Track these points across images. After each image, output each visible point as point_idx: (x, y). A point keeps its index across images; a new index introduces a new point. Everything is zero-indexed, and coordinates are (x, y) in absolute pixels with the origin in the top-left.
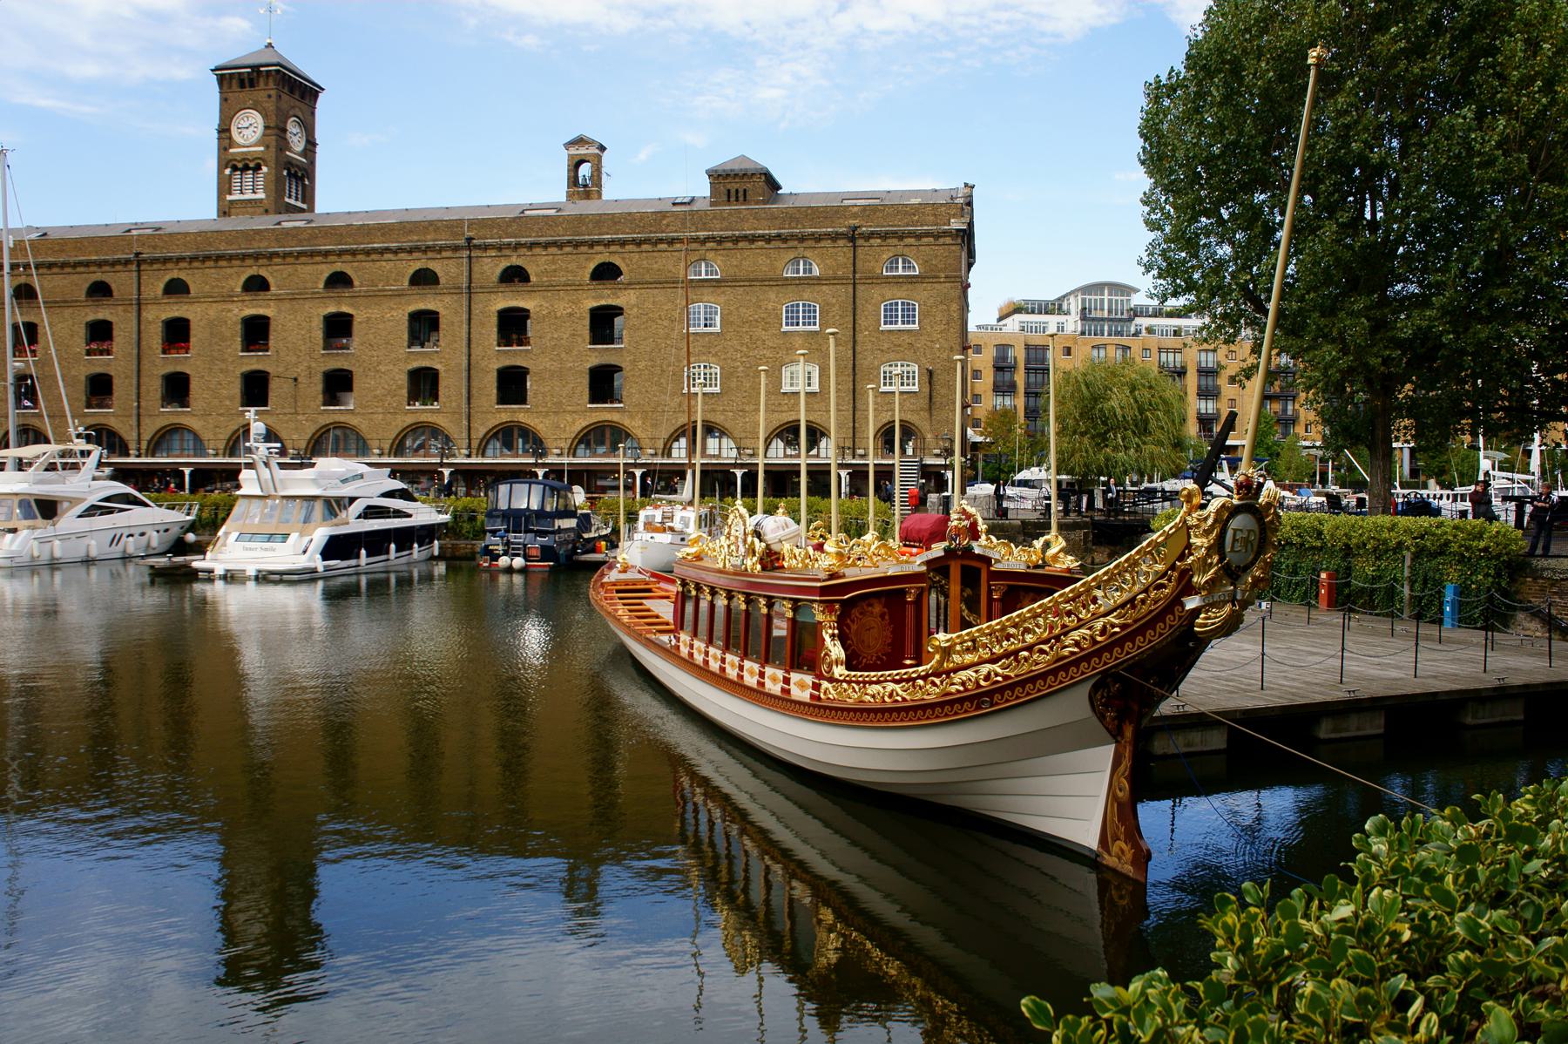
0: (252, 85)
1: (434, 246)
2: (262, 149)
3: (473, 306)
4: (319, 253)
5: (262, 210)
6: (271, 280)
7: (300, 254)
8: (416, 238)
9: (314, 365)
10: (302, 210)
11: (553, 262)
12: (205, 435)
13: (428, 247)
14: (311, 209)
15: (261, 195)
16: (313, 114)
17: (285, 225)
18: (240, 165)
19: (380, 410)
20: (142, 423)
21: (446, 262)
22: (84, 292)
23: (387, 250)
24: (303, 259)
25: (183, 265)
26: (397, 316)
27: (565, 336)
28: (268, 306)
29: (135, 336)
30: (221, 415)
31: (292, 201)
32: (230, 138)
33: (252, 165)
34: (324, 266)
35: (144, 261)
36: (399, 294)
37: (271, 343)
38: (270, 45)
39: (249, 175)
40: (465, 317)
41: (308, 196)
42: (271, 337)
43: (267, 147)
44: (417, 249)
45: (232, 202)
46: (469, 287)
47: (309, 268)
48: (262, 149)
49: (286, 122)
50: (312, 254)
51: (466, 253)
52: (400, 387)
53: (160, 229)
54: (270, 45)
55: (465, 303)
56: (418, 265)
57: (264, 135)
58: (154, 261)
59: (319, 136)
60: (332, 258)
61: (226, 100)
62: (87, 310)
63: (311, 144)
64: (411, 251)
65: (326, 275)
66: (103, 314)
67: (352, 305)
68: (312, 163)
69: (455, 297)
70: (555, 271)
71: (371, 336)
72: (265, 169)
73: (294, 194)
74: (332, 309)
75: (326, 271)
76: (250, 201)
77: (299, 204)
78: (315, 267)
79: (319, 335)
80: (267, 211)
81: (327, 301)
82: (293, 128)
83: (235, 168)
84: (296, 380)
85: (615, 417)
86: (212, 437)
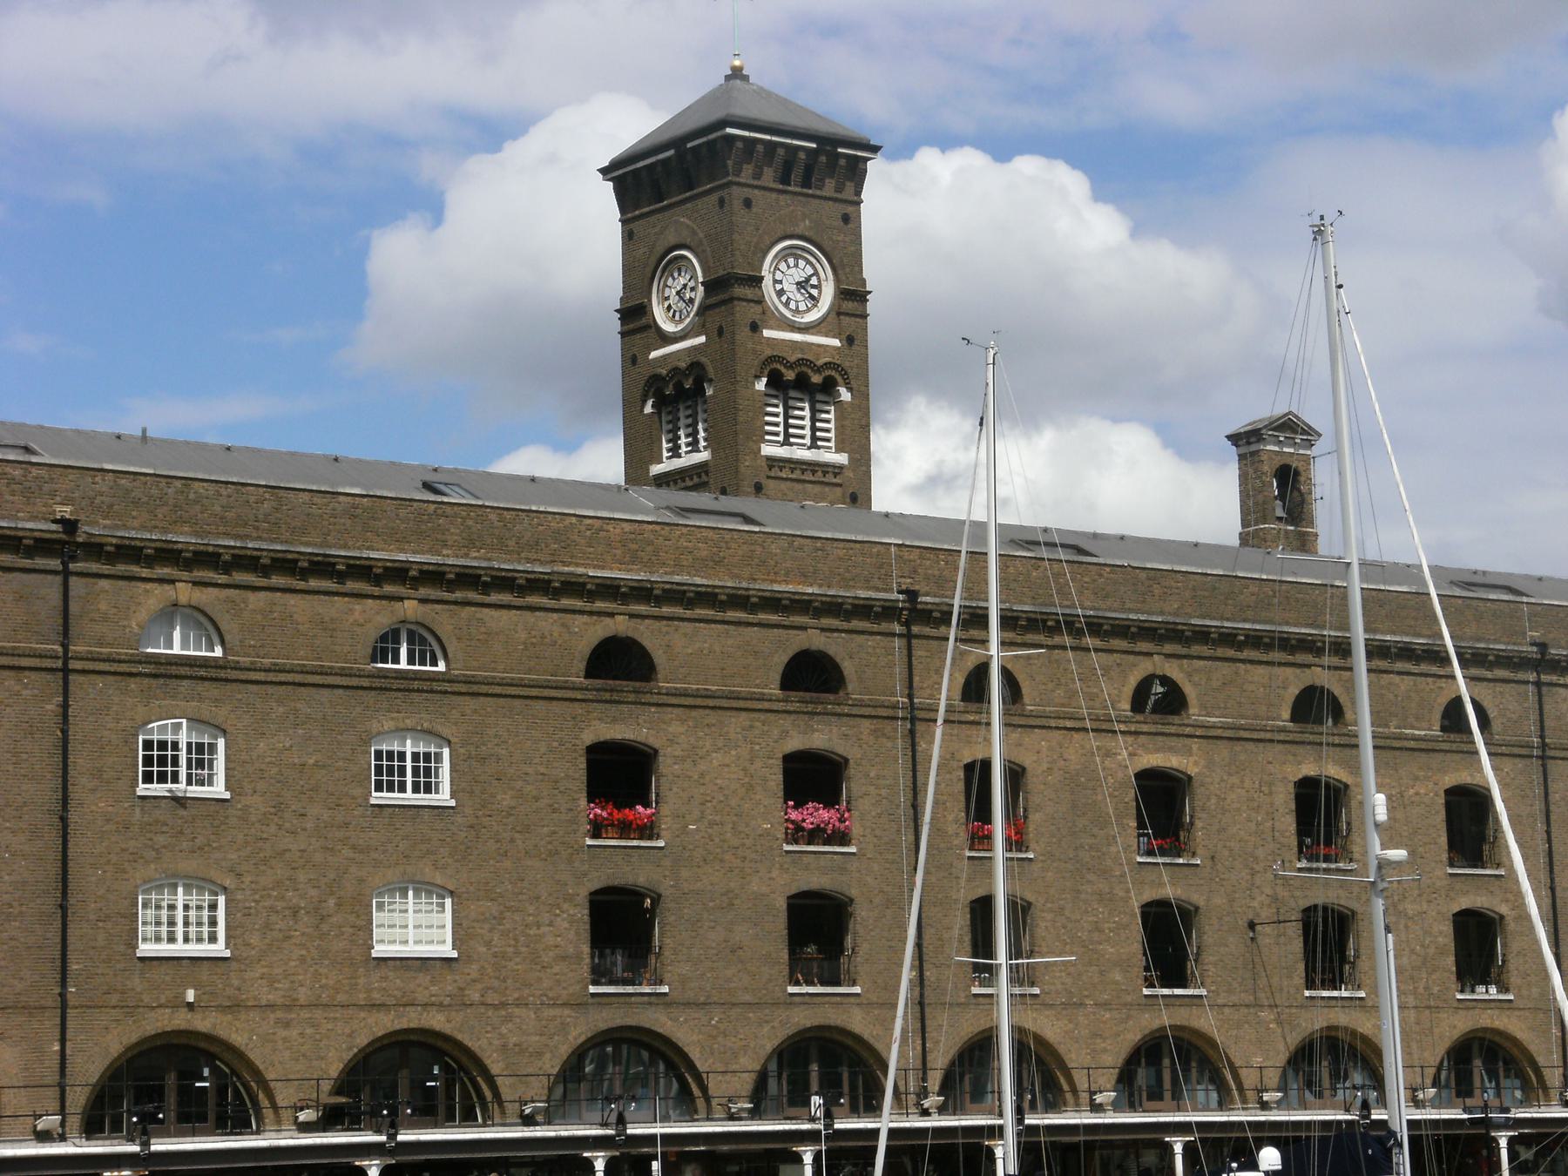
0: (806, 183)
2: (836, 342)
3: (1552, 787)
6: (1189, 690)
18: (790, 375)
21: (1499, 687)
22: (776, 677)
29: (903, 799)
30: (1105, 1005)
32: (760, 301)
33: (816, 379)
38: (737, 74)
45: (772, 461)
46: (1544, 746)
48: (836, 342)
51: (1532, 677)
54: (737, 74)
55: (1537, 777)
62: (786, 722)
65: (1294, 691)
66: (821, 737)
74: (1309, 770)
81: (1300, 749)
83: (775, 381)
86: (1087, 1061)
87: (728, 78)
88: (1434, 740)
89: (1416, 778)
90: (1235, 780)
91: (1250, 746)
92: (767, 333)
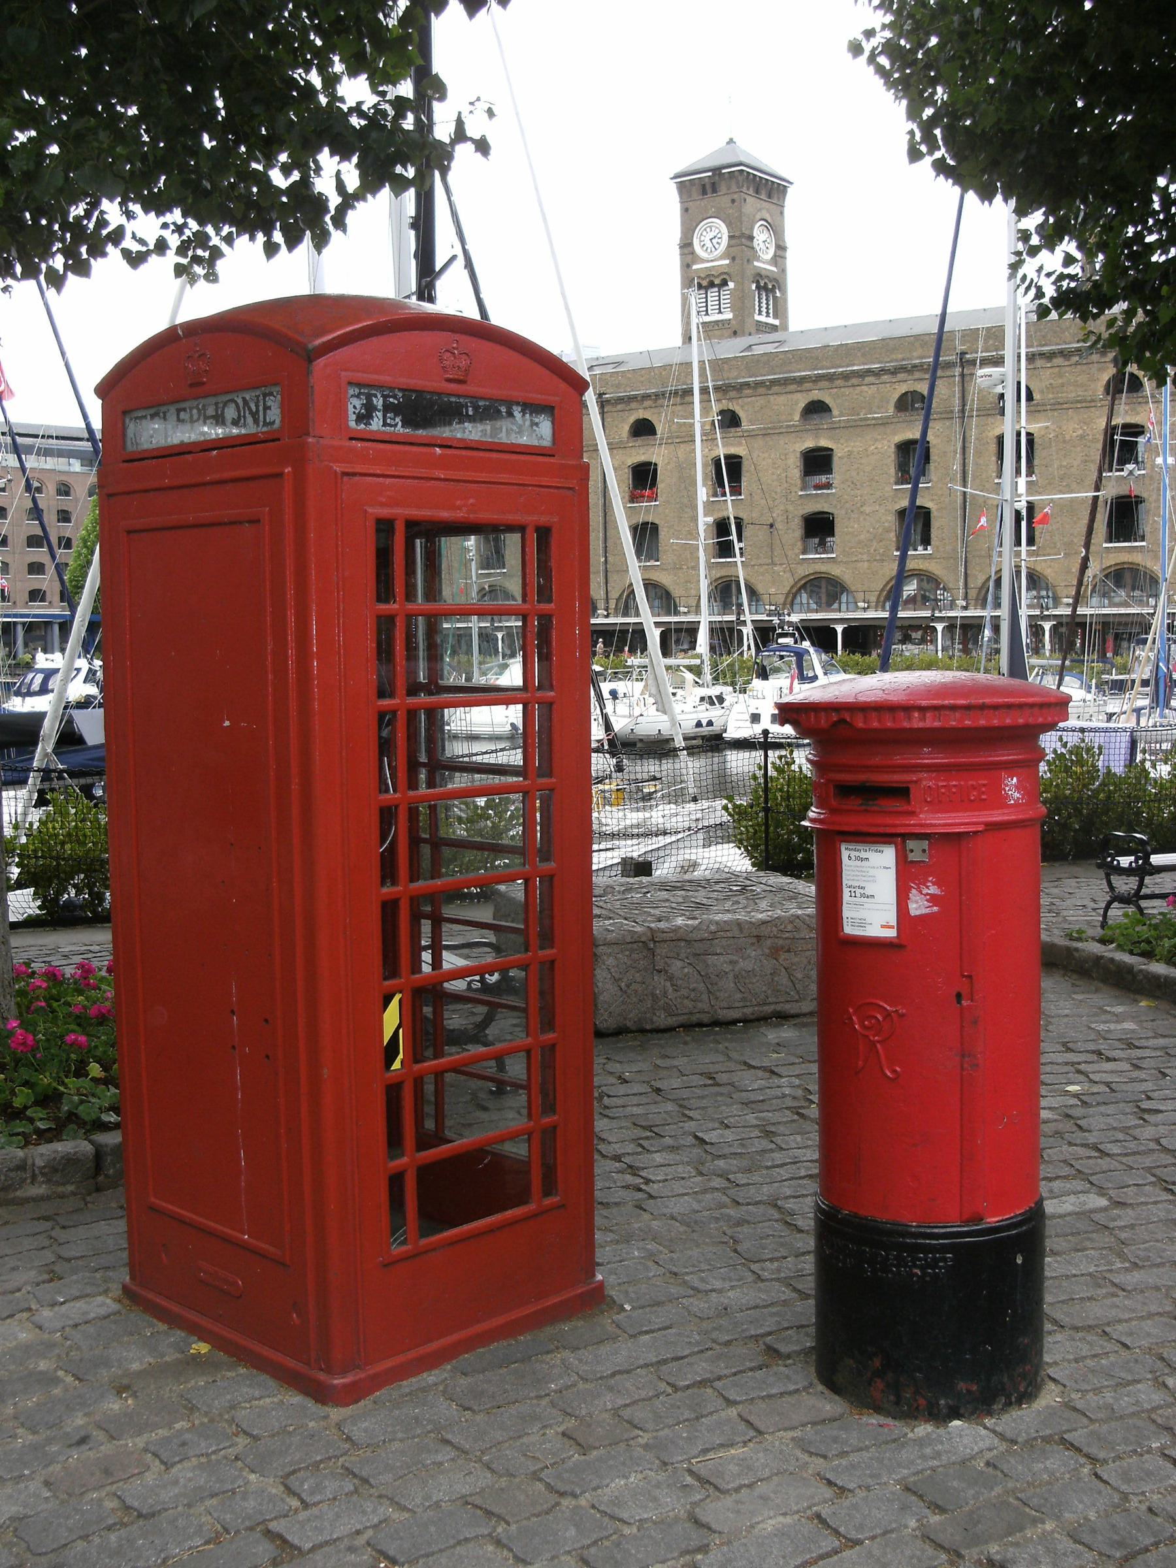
0: (714, 191)
1: (922, 365)
2: (727, 262)
4: (794, 380)
5: (730, 332)
6: (741, 414)
7: (773, 382)
8: (900, 356)
9: (791, 508)
10: (774, 328)
11: (1060, 376)
12: (676, 592)
13: (915, 366)
14: (784, 327)
15: (728, 315)
16: (782, 213)
17: (759, 350)
18: (705, 283)
19: (865, 557)
20: (610, 580)
23: (869, 372)
24: (776, 389)
25: (648, 403)
26: (884, 447)
27: (1075, 463)
28: (740, 444)
31: (763, 318)
32: (693, 253)
33: (717, 282)
34: (799, 395)
35: (608, 401)
36: (884, 423)
37: (743, 484)
39: (713, 294)
40: (959, 445)
41: (779, 310)
42: (743, 479)
43: (733, 259)
44: (903, 369)
46: (963, 411)
47: (782, 399)
48: (727, 262)
49: (752, 229)
50: (785, 382)
52: (888, 531)
53: (619, 364)
54: (731, 141)
56: (903, 388)
57: (729, 246)
58: (620, 400)
59: (790, 239)
60: (808, 385)
61: (686, 210)
63: (781, 248)
64: (894, 372)
65: (802, 405)
67: (831, 438)
68: (783, 271)
69: (948, 423)
70: (1062, 385)
71: (854, 474)
72: (731, 285)
73: (764, 310)
74: (810, 444)
75: (802, 401)
76: (717, 322)
77: (771, 321)
78: (790, 396)
79: (796, 472)
80: (735, 333)
82: (761, 236)
84: (771, 526)
85: (1137, 558)
87: (728, 143)
88: (888, 417)
89: (876, 440)
90: (766, 455)
91: (776, 437)
92: (695, 267)
